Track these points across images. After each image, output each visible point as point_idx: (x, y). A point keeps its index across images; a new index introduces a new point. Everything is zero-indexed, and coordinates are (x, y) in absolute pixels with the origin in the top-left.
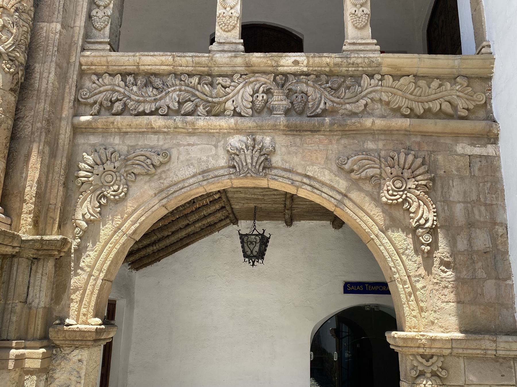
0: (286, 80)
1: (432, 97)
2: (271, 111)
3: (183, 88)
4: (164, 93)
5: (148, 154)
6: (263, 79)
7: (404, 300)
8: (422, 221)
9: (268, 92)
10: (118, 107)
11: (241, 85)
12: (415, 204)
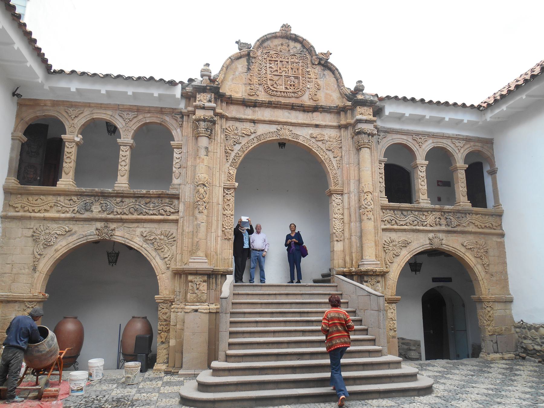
1: (487, 222)
3: (414, 216)
4: (407, 218)
6: (438, 213)
7: (481, 286)
8: (486, 263)
9: (440, 218)
10: (393, 222)
11: (431, 215)
12: (484, 257)
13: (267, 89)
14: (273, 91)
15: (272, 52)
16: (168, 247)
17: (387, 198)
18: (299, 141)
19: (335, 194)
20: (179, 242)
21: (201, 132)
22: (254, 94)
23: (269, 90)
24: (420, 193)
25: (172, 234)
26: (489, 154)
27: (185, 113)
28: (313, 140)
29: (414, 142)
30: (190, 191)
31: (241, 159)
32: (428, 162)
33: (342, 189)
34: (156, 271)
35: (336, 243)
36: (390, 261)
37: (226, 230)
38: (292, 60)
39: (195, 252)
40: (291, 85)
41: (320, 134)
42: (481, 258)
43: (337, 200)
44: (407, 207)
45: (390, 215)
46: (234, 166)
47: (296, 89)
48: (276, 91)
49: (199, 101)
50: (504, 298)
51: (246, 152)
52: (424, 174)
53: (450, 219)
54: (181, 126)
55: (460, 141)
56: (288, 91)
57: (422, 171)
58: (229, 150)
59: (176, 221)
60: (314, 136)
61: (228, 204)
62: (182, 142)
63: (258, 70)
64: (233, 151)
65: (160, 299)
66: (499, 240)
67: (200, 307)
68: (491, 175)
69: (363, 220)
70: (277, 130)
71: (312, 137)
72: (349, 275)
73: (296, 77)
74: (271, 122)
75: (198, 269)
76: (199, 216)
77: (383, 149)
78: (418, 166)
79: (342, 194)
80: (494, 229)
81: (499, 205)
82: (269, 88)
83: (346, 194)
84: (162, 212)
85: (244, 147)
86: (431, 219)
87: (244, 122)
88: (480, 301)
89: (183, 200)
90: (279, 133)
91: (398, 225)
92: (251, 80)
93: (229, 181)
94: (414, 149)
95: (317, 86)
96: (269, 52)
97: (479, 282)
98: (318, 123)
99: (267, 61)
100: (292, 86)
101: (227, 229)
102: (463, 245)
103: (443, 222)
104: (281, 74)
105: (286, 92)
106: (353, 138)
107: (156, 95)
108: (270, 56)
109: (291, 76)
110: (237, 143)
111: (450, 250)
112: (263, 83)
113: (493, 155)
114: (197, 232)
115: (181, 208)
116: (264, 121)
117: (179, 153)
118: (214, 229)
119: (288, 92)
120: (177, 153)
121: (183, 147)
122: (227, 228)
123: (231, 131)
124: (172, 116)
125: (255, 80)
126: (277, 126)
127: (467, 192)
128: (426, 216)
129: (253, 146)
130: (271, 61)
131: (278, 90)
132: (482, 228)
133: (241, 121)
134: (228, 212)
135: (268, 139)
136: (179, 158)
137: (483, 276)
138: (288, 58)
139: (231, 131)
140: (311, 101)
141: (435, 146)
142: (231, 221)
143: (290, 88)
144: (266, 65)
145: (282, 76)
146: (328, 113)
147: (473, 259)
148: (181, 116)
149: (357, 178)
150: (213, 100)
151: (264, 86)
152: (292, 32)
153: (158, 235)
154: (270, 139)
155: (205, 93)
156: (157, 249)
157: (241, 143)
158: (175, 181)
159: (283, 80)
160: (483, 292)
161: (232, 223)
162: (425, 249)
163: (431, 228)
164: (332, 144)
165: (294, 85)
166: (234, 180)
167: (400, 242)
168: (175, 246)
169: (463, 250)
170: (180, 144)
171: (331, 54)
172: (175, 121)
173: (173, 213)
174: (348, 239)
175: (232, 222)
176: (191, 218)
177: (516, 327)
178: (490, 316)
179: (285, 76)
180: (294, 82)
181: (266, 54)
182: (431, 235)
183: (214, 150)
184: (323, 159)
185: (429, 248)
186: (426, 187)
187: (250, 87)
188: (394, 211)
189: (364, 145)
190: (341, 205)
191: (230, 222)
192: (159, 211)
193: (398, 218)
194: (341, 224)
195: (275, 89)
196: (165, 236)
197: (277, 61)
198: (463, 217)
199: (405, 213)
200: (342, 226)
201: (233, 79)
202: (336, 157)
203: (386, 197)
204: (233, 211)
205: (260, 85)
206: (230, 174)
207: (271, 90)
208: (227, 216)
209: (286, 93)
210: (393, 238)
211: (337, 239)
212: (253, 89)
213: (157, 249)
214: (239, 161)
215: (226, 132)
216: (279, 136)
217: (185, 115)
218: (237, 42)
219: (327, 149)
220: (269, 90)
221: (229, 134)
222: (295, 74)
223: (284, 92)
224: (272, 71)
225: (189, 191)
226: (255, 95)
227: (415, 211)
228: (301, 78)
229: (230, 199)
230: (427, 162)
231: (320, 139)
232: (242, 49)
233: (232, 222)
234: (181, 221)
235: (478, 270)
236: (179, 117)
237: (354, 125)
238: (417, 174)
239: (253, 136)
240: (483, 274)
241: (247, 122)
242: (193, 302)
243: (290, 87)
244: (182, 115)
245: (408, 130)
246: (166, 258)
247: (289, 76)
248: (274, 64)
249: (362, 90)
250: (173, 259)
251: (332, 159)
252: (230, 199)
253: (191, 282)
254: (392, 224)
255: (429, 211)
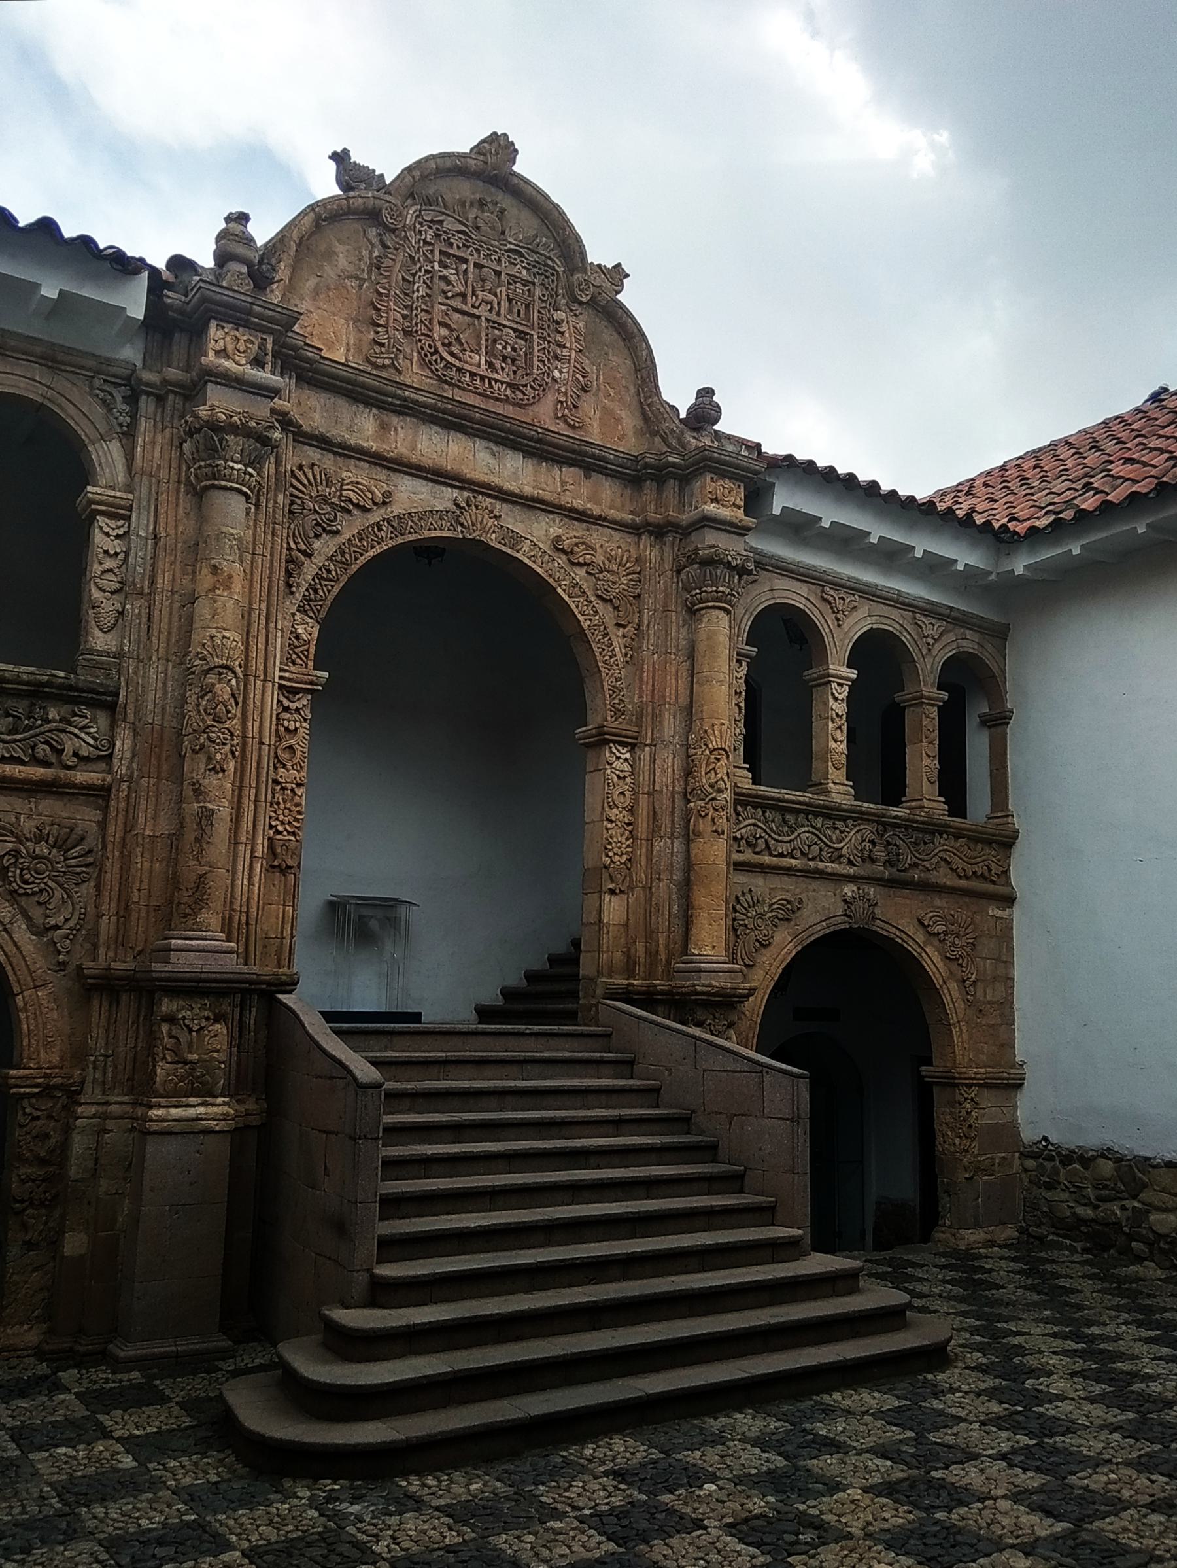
0: (885, 831)
1: (978, 860)
2: (873, 861)
3: (812, 830)
4: (796, 834)
5: (788, 898)
9: (872, 842)
11: (853, 832)
13: (432, 354)
14: (448, 365)
15: (449, 224)
16: (64, 889)
17: (748, 770)
18: (519, 556)
19: (614, 742)
20: (112, 870)
21: (228, 472)
22: (387, 362)
23: (436, 361)
24: (830, 763)
25: (83, 838)
26: (995, 669)
27: (148, 384)
28: (562, 560)
29: (826, 608)
30: (165, 684)
31: (336, 590)
32: (856, 672)
33: (636, 729)
34: (12, 977)
35: (607, 897)
36: (747, 961)
37: (278, 837)
38: (514, 271)
39: (188, 911)
40: (504, 359)
41: (583, 543)
42: (960, 961)
43: (618, 765)
44: (800, 803)
45: (752, 821)
46: (311, 614)
47: (520, 373)
48: (459, 370)
49: (217, 353)
50: (1005, 1075)
51: (354, 568)
52: (840, 708)
53: (895, 845)
54: (128, 435)
55: (933, 621)
56: (496, 376)
57: (840, 697)
58: (299, 550)
59: (100, 794)
60: (566, 544)
61: (290, 742)
62: (130, 496)
63: (404, 279)
64: (309, 556)
65: (28, 1082)
66: (999, 913)
67: (201, 1110)
68: (990, 727)
69: (698, 834)
70: (454, 508)
71: (558, 549)
72: (648, 1000)
73: (521, 332)
74: (438, 476)
75: (203, 976)
76: (211, 782)
77: (747, 617)
78: (830, 682)
79: (632, 747)
80: (993, 882)
81: (1007, 816)
82: (436, 351)
83: (647, 749)
84: (42, 750)
85: (347, 550)
86: (851, 840)
87: (350, 457)
88: (951, 1082)
89: (131, 717)
90: (462, 520)
91: (771, 855)
92: (379, 310)
93: (294, 663)
94: (825, 631)
95: (581, 379)
96: (441, 222)
97: (950, 1030)
98: (578, 504)
99: (432, 251)
100: (509, 361)
101: (280, 833)
102: (921, 922)
103: (879, 853)
104: (475, 311)
105: (490, 379)
106: (679, 572)
107: (50, 291)
108: (444, 236)
109: (505, 326)
110: (324, 529)
111: (892, 936)
112: (416, 332)
113: (1003, 672)
114: (198, 840)
115: (123, 744)
116: (419, 468)
117: (118, 537)
118: (247, 832)
119: (496, 381)
120: (107, 534)
121: (134, 514)
122: (280, 828)
123: (306, 482)
124: (92, 388)
125: (395, 313)
126: (456, 493)
127: (940, 771)
128: (842, 832)
129: (378, 550)
130: (448, 255)
131: (466, 367)
132: (967, 878)
133: (340, 455)
134: (287, 775)
135: (428, 534)
136: (116, 554)
137: (961, 1016)
138: (499, 261)
139: (306, 483)
140: (562, 425)
141: (875, 626)
142: (298, 805)
143: (503, 369)
144: (429, 268)
145: (479, 317)
146: (607, 475)
147: (940, 965)
148: (129, 393)
149: (683, 701)
150: (269, 358)
151: (420, 340)
152: (515, 168)
153: (27, 839)
154: (434, 534)
155: (241, 329)
156: (21, 891)
157: (337, 532)
158: (100, 641)
159: (483, 334)
160: (959, 1059)
161: (299, 813)
162: (832, 929)
163: (851, 871)
164: (614, 583)
165: (513, 360)
166: (311, 663)
167: (775, 906)
168: (92, 884)
169: (920, 938)
170: (123, 502)
171: (627, 276)
172: (100, 410)
173: (86, 759)
174: (644, 888)
175: (298, 809)
176: (166, 785)
177: (1024, 1155)
178: (970, 1126)
179: (488, 320)
180: (514, 349)
181: (430, 227)
182: (849, 890)
183: (254, 544)
184: (585, 625)
185: (842, 927)
186: (844, 746)
187: (372, 335)
188: (764, 812)
189: (718, 600)
190: (628, 780)
191: (293, 808)
192: (33, 748)
193: (774, 832)
194: (627, 839)
195: (457, 363)
196: (53, 847)
197: (466, 261)
198: (925, 843)
199: (790, 818)
200: (628, 846)
201: (316, 292)
202: (624, 626)
203: (747, 766)
204: (304, 773)
205: (407, 333)
206: (298, 637)
207: (444, 363)
208: (283, 789)
209: (490, 383)
210: (757, 891)
211: (612, 886)
212: (383, 345)
213: (20, 895)
214: (331, 597)
215: (292, 485)
216: (460, 528)
217: (148, 394)
218: (335, 157)
219: (599, 597)
220: (436, 361)
221: (301, 495)
222: (518, 320)
223: (483, 378)
224: (450, 294)
225: (160, 684)
226: (392, 370)
227: (816, 815)
228: (535, 336)
229: (296, 729)
230: (853, 674)
231: (581, 560)
232: (353, 189)
233: (298, 809)
234: (123, 795)
235: (951, 994)
236: (119, 399)
237: (686, 531)
238: (826, 703)
239: (376, 516)
240: (960, 1005)
241: (360, 459)
242: (176, 1095)
243: (503, 365)
244: (134, 392)
245: (814, 569)
246: (56, 927)
247: (500, 324)
248: (456, 269)
249: (717, 421)
250: (83, 932)
251: (612, 629)
252: (296, 729)
253: (171, 1019)
254: (757, 850)
255: (850, 817)
